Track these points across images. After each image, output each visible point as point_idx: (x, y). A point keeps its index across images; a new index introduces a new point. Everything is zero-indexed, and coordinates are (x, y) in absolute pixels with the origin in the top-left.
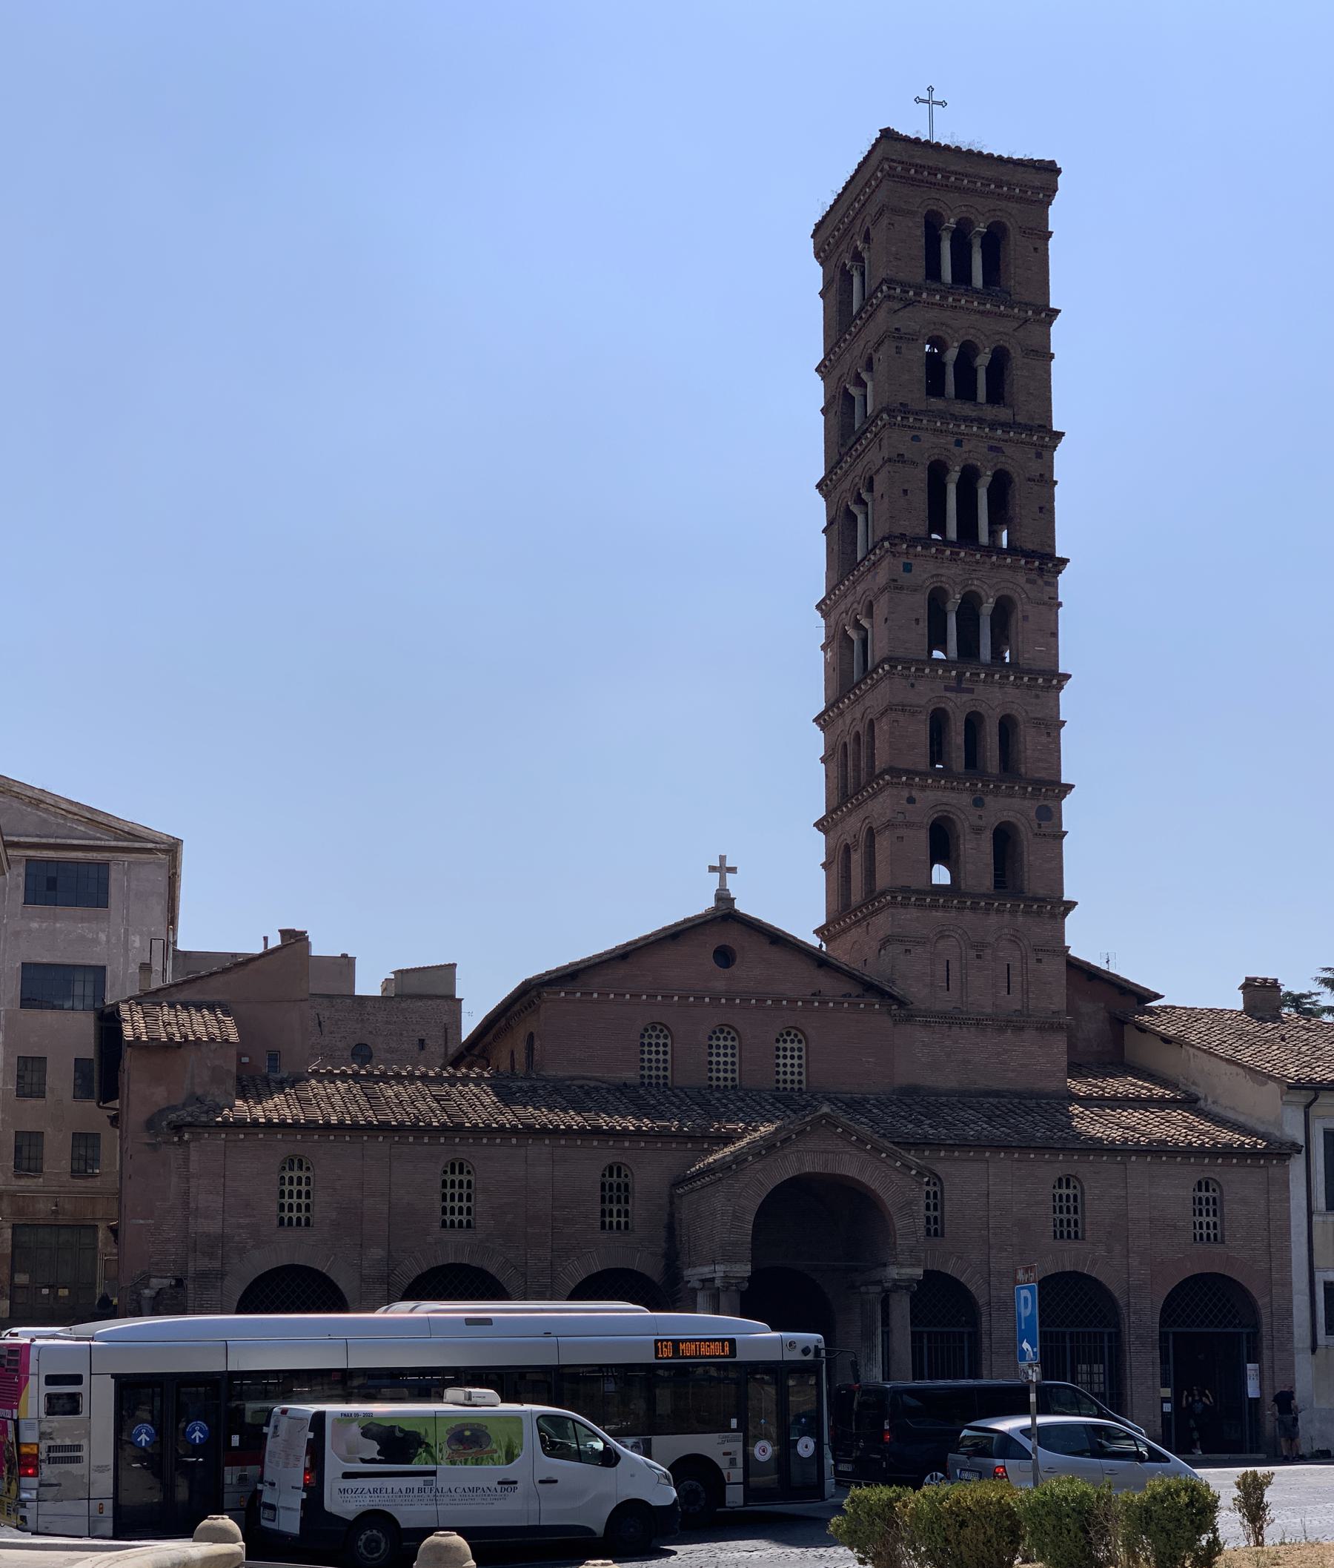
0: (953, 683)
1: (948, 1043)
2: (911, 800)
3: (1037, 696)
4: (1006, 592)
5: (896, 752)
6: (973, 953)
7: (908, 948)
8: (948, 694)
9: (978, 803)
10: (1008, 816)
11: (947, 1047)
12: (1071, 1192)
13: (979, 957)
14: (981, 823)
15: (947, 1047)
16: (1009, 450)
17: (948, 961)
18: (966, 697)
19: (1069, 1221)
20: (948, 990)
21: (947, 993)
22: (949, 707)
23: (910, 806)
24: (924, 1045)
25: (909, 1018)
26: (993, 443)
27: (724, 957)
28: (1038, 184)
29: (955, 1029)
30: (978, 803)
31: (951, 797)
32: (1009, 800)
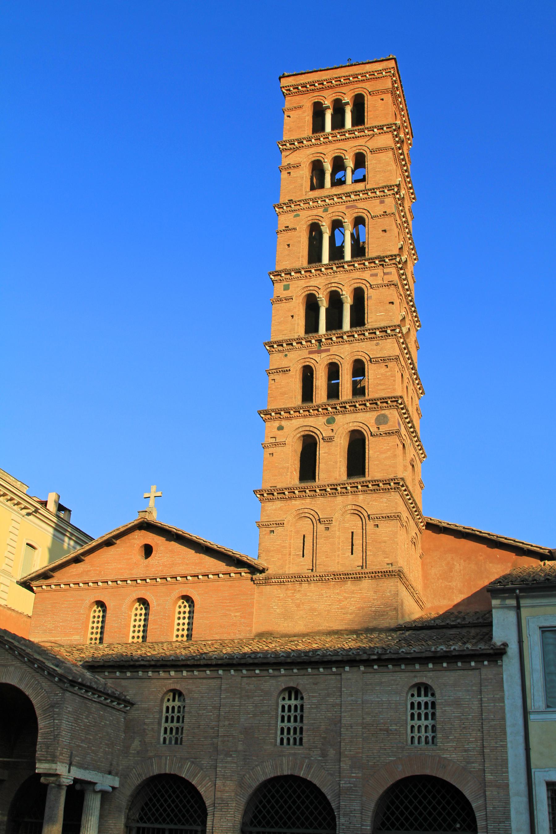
0: (315, 348)
1: (298, 596)
2: (280, 428)
3: (377, 344)
4: (356, 286)
5: (273, 399)
6: (321, 527)
7: (272, 529)
8: (311, 356)
9: (330, 421)
10: (353, 427)
11: (298, 599)
12: (298, 702)
13: (327, 529)
14: (332, 434)
15: (298, 599)
16: (360, 205)
17: (304, 535)
18: (324, 355)
19: (289, 729)
20: (303, 556)
21: (302, 559)
22: (311, 363)
23: (280, 432)
24: (278, 600)
25: (267, 581)
26: (349, 204)
27: (148, 550)
28: (381, 69)
29: (305, 585)
30: (330, 421)
31: (311, 421)
32: (354, 415)
